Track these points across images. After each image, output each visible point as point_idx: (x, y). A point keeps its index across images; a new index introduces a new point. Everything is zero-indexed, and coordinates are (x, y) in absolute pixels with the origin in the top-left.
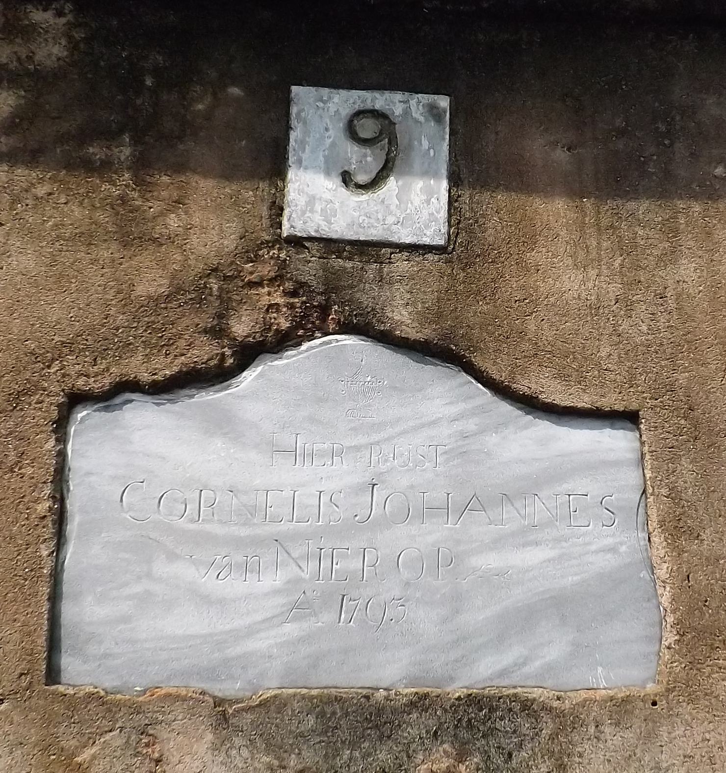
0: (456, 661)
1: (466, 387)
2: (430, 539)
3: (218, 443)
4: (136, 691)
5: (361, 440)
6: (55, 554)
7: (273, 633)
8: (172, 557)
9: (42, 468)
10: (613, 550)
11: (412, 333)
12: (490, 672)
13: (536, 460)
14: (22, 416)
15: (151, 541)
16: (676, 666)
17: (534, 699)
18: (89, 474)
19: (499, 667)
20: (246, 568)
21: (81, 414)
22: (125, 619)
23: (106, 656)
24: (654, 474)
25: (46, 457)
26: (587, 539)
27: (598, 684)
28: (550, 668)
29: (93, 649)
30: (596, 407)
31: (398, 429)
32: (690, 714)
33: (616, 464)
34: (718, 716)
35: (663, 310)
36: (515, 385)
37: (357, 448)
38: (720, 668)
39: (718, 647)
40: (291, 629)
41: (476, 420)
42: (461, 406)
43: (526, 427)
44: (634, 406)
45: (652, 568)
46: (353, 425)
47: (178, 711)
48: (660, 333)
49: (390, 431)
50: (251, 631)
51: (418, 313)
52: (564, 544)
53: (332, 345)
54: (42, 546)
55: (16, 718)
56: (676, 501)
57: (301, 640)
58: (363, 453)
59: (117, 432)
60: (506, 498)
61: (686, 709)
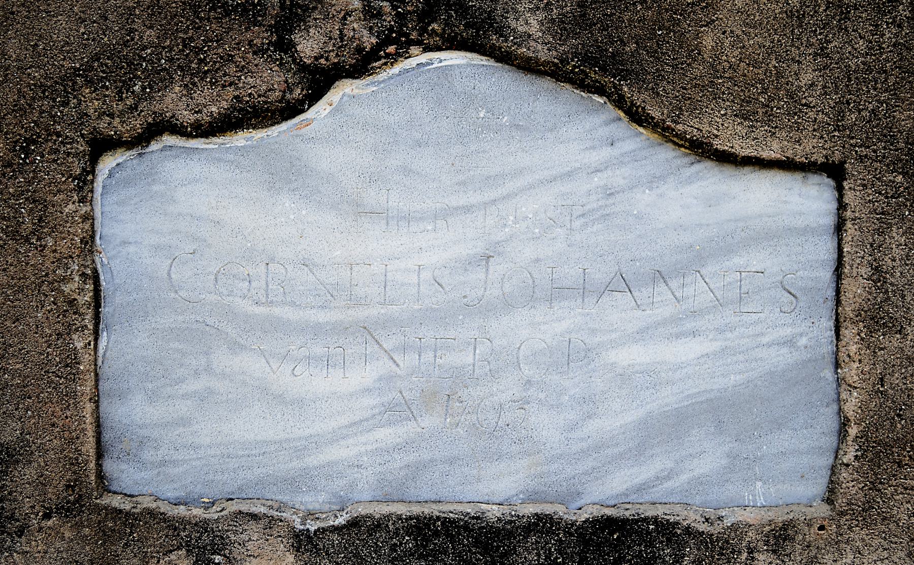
0: (585, 473)
1: (613, 127)
2: (560, 327)
3: (286, 202)
4: (204, 502)
5: (472, 198)
6: (92, 347)
7: (363, 439)
8: (236, 347)
9: (64, 239)
10: (790, 343)
11: (544, 54)
12: (625, 487)
13: (700, 225)
14: (34, 171)
15: (208, 328)
16: (853, 486)
17: (677, 523)
18: (125, 243)
19: (638, 481)
20: (328, 362)
21: (108, 163)
22: (184, 422)
23: (163, 463)
24: (854, 249)
25: (68, 225)
26: (758, 329)
27: (755, 500)
28: (699, 482)
29: (148, 455)
30: (787, 158)
31: (520, 183)
32: (863, 540)
33: (805, 231)
34: (896, 543)
35: (891, 20)
36: (680, 127)
37: (467, 209)
38: (906, 489)
39: (906, 465)
40: (386, 435)
41: (625, 171)
42: (606, 153)
43: (689, 181)
44: (837, 157)
45: (837, 365)
46: (461, 177)
47: (254, 531)
48: (881, 54)
49: (511, 186)
50: (336, 438)
51: (553, 21)
52: (729, 335)
53: (434, 66)
54: (75, 337)
55: (67, 534)
56: (879, 284)
57: (398, 448)
58: (475, 214)
59: (155, 188)
60: (660, 276)
61: (859, 535)
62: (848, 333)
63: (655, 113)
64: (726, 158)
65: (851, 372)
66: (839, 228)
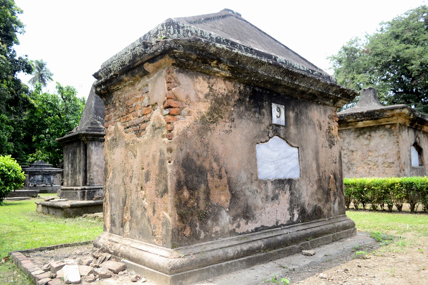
22: (263, 171)
29: (261, 174)
62: (300, 161)
63: (289, 142)
64: (292, 146)
65: (301, 165)
66: (299, 152)
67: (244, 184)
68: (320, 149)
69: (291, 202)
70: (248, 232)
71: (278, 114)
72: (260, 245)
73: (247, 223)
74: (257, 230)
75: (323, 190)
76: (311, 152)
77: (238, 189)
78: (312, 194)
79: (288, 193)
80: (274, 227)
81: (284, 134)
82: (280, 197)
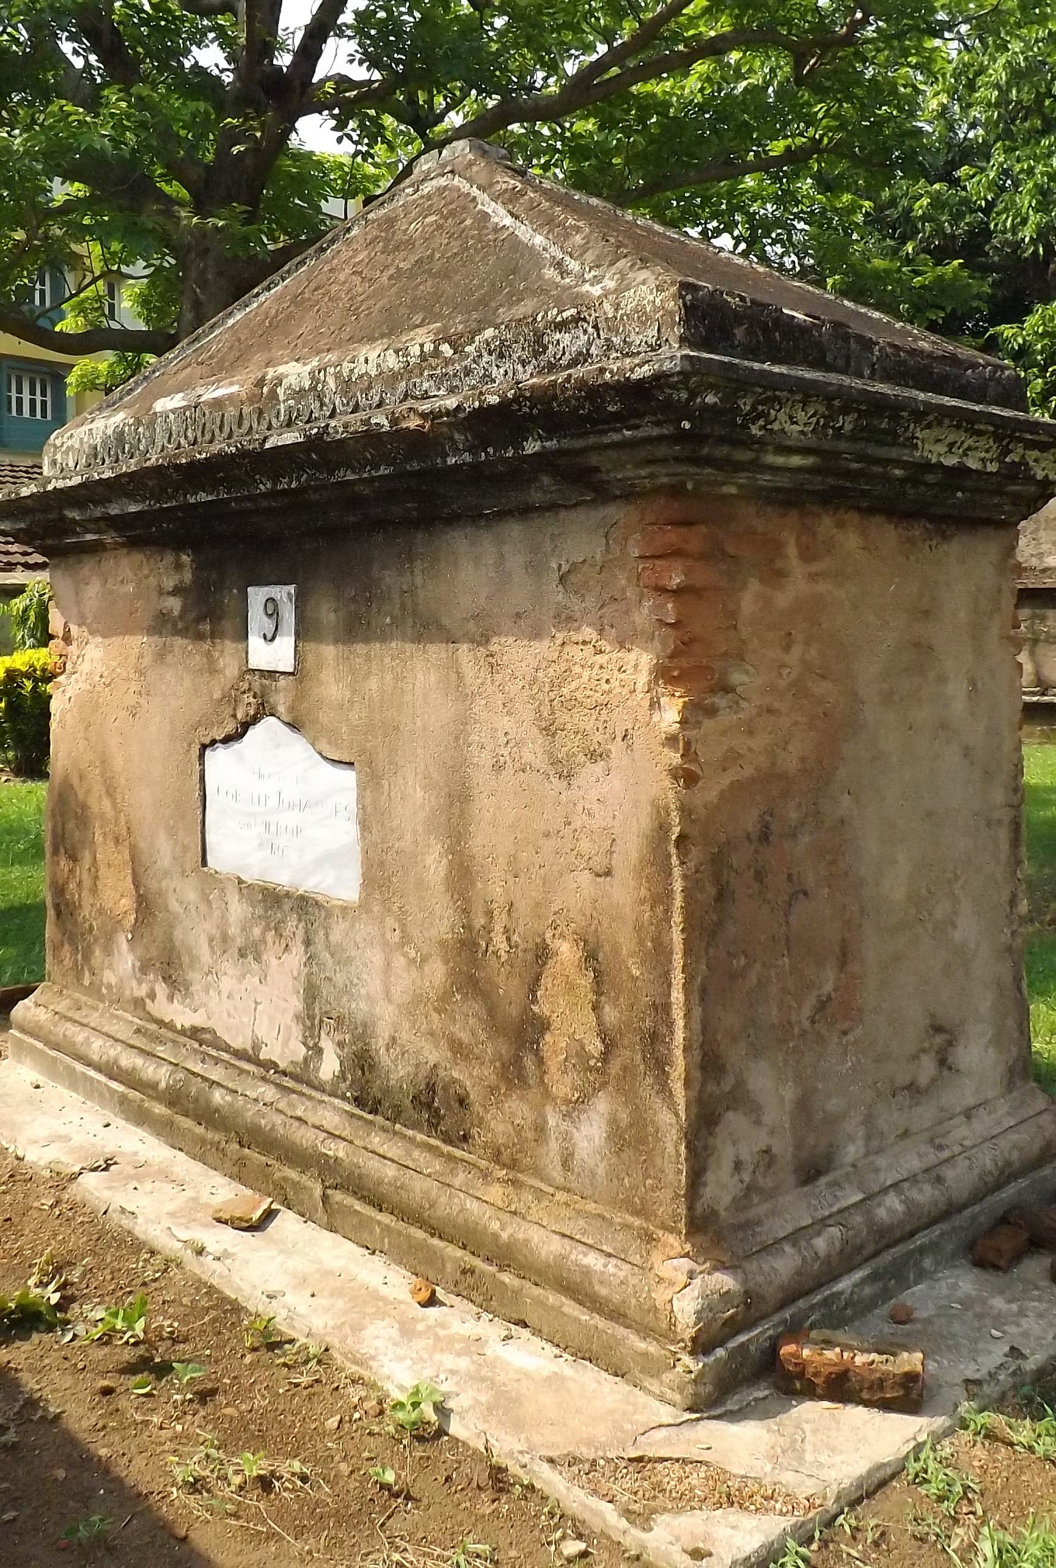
67: (166, 873)
68: (481, 778)
69: (311, 993)
70: (169, 1026)
71: (269, 625)
72: (157, 1078)
73: (171, 998)
74: (194, 1033)
75: (492, 1010)
76: (420, 793)
77: (153, 885)
78: (418, 999)
79: (297, 954)
80: (239, 1054)
81: (292, 709)
82: (269, 957)
